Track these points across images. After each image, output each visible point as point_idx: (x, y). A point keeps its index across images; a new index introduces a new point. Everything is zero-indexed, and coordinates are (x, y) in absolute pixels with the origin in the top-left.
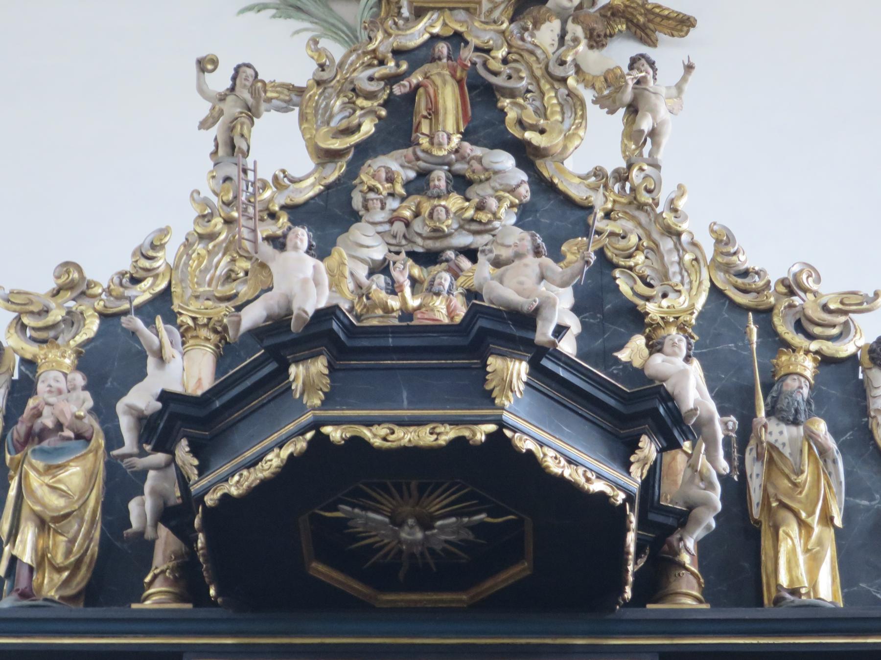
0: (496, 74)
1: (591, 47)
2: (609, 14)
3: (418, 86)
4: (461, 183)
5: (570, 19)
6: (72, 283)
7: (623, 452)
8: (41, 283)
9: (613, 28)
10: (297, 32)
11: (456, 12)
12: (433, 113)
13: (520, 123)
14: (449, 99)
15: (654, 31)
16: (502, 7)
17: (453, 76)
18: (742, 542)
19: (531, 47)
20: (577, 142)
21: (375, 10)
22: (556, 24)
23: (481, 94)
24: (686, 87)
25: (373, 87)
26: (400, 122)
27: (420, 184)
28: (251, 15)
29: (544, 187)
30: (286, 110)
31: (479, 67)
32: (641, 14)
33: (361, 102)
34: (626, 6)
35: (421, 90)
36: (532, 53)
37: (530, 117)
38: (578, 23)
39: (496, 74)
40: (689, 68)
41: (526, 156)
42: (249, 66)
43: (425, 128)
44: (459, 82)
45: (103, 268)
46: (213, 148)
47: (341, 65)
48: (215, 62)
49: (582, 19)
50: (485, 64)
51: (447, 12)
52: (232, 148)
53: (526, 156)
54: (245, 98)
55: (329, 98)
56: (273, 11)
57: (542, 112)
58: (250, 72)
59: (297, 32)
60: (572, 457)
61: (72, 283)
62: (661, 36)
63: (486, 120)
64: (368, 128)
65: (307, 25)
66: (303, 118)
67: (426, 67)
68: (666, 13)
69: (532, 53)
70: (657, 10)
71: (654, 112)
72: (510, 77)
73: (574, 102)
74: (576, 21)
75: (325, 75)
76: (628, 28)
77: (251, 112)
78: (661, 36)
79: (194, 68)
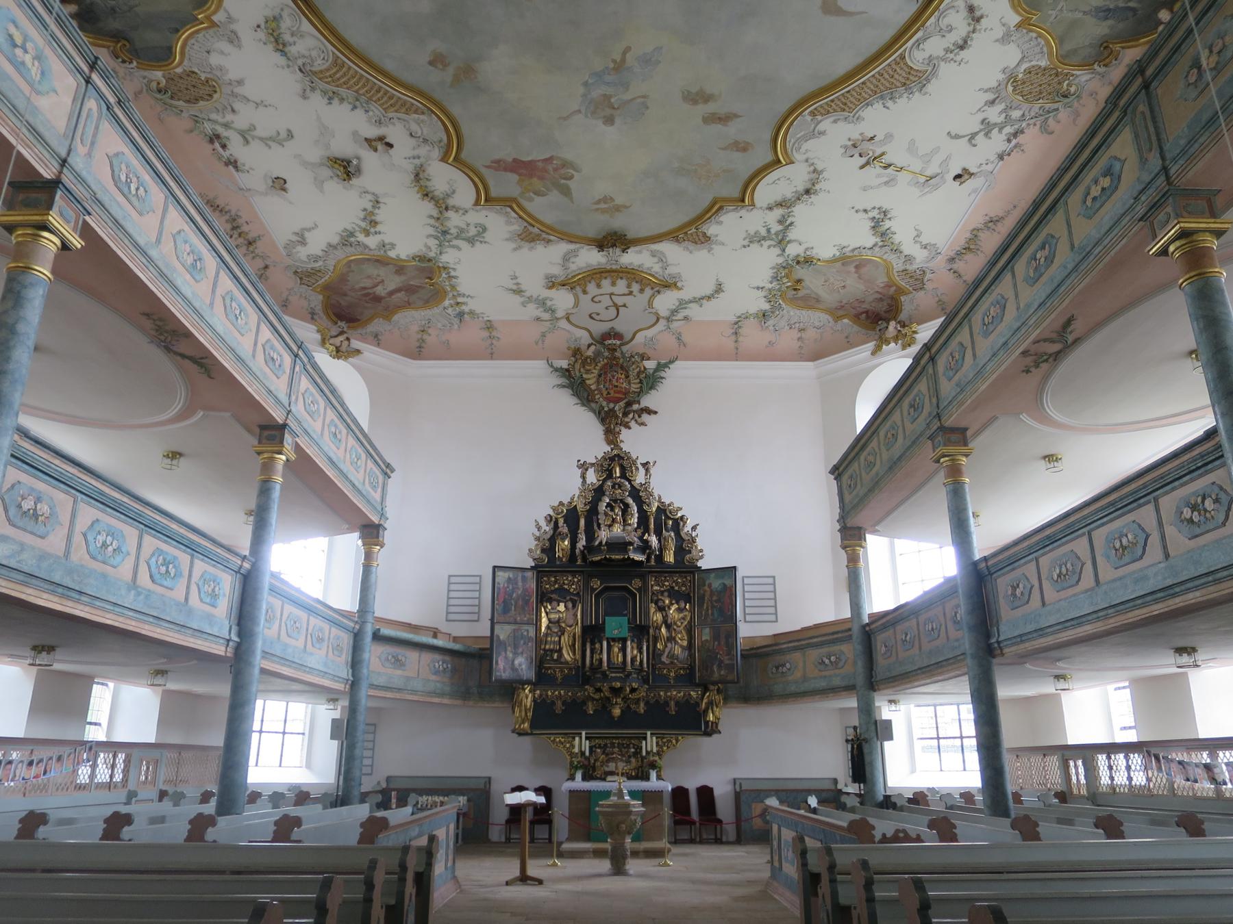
4: (620, 487)
6: (561, 504)
7: (644, 553)
8: (556, 504)
18: (660, 558)
26: (610, 475)
27: (613, 487)
29: (632, 486)
41: (630, 481)
45: (566, 502)
52: (583, 477)
53: (630, 481)
54: (584, 467)
60: (639, 557)
61: (561, 504)
63: (623, 476)
73: (637, 469)
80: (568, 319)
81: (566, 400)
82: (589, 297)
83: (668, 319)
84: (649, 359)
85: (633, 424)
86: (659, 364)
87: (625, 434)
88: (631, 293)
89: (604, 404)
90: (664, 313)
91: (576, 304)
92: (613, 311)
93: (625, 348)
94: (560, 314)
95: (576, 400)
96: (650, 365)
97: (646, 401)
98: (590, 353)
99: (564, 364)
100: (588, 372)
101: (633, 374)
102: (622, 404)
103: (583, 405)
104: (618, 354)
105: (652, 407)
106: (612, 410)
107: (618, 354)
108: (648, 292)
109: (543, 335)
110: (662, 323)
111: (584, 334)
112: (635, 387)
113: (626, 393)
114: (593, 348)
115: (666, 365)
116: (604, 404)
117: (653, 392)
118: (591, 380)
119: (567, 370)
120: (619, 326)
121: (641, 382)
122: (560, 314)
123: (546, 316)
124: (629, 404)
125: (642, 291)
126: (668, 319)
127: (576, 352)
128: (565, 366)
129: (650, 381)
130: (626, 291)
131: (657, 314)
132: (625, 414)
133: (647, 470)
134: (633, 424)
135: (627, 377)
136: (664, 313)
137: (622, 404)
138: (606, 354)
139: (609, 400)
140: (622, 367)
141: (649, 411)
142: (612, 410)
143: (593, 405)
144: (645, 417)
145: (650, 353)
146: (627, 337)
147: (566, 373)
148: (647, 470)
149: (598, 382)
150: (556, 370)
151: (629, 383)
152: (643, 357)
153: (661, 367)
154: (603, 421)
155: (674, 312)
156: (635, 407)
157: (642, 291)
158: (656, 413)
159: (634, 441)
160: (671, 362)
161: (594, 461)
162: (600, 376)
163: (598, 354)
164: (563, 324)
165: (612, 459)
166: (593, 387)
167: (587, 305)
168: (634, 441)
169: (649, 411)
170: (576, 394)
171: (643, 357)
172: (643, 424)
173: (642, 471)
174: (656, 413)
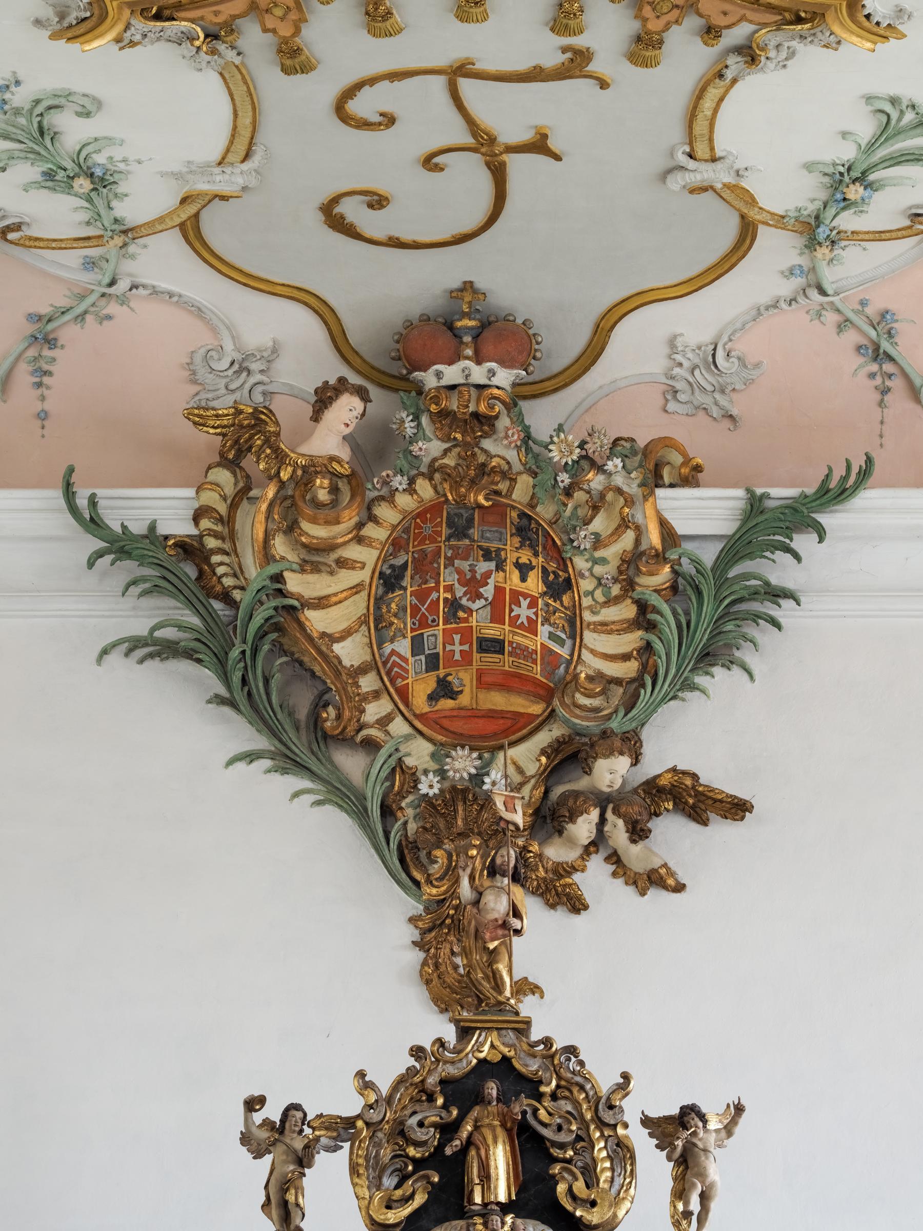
0: (545, 1125)
1: (634, 841)
2: (654, 791)
3: (469, 1142)
5: (611, 806)
9: (659, 806)
10: (296, 795)
11: (504, 1032)
12: (486, 1177)
13: (574, 1197)
14: (500, 1159)
15: (705, 811)
16: (533, 781)
17: (503, 1125)
19: (578, 1079)
20: (627, 1205)
21: (387, 784)
22: (595, 814)
23: (530, 1145)
24: (738, 1130)
25: (420, 1135)
28: (241, 766)
30: (336, 1149)
31: (529, 1117)
32: (690, 796)
33: (411, 1151)
34: (673, 785)
35: (473, 1152)
36: (582, 1088)
37: (579, 1186)
38: (619, 816)
39: (545, 1125)
40: (739, 1109)
42: (296, 1107)
43: (478, 1199)
44: (509, 1131)
46: (263, 1199)
47: (389, 1100)
48: (262, 1100)
49: (623, 809)
50: (535, 1111)
51: (495, 1033)
55: (379, 1145)
56: (267, 763)
57: (591, 1181)
58: (299, 1115)
59: (296, 795)
62: (712, 816)
64: (420, 1199)
65: (306, 784)
66: (354, 1170)
67: (475, 1112)
68: (720, 797)
69: (582, 1088)
70: (711, 794)
71: (702, 1175)
72: (560, 1128)
73: (623, 1153)
74: (616, 812)
75: (374, 1115)
76: (675, 804)
77: (303, 1160)
78: (712, 816)
79: (241, 1108)
80: (192, 233)
81: (182, 729)
82: (318, 90)
83: (811, 231)
84: (691, 476)
85: (594, 879)
86: (755, 505)
87: (542, 946)
88: (577, 64)
89: (419, 754)
90: (784, 189)
91: (244, 143)
92: (469, 178)
93: (542, 416)
94: (144, 197)
95: (243, 734)
96: (701, 513)
97: (684, 737)
98: (330, 438)
99: (170, 510)
100: (316, 557)
101: (592, 571)
102: (528, 754)
103: (288, 762)
104: (500, 448)
105: (718, 776)
106: (468, 796)
107: (500, 448)
108: (687, 52)
109: (43, 335)
110: (775, 250)
111: (297, 326)
112: (606, 650)
113: (555, 688)
114: (346, 411)
115: (801, 517)
116: (419, 754)
117: (720, 681)
118: (336, 611)
119: (189, 549)
120: (506, 272)
121: (644, 618)
122: (144, 197)
123: (58, 214)
124: (570, 756)
125: (645, 48)
126: (811, 231)
127: (246, 437)
128: (177, 524)
129: (710, 613)
130: (548, 50)
131: (738, 196)
132: (549, 818)
133: (687, 1164)
134: (594, 879)
135: (560, 586)
136: (784, 189)
137: (528, 754)
138: (431, 448)
139: (447, 734)
140: (527, 529)
141: (698, 801)
142: (468, 796)
143: (351, 764)
144: (673, 838)
145: (698, 439)
146: (562, 344)
147: (182, 565)
148: (687, 1164)
149: (378, 623)
150: (121, 546)
151: (574, 627)
152: (658, 466)
153: (770, 525)
154: (406, 861)
155: (847, 182)
156: (611, 772)
157: (645, 48)
158: (737, 809)
159: (599, 983)
160: (835, 493)
161: (349, 1104)
162: (390, 580)
163: (375, 447)
164: (164, 262)
165: (463, 1092)
166: (350, 652)
167: (309, 152)
168: (599, 983)
169: (698, 801)
170: (244, 695)
171: (658, 466)
172: (656, 880)
173: (654, 1167)
174: (737, 809)
